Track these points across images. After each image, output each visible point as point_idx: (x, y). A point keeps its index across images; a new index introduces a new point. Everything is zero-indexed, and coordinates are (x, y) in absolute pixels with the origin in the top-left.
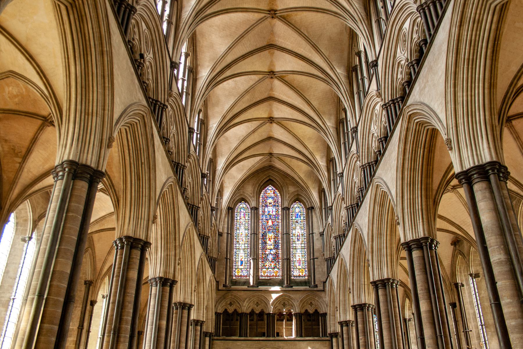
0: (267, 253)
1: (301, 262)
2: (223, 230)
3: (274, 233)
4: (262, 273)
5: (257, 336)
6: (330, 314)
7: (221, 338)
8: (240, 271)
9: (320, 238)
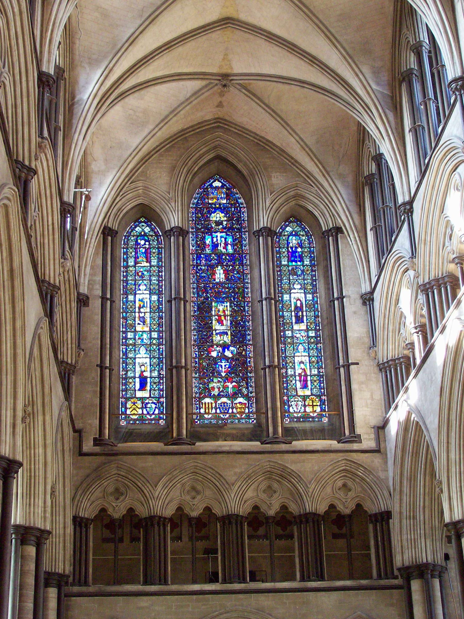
0: (214, 354)
1: (309, 378)
5: (194, 582)
6: (401, 513)
7: (92, 589)
8: (139, 404)
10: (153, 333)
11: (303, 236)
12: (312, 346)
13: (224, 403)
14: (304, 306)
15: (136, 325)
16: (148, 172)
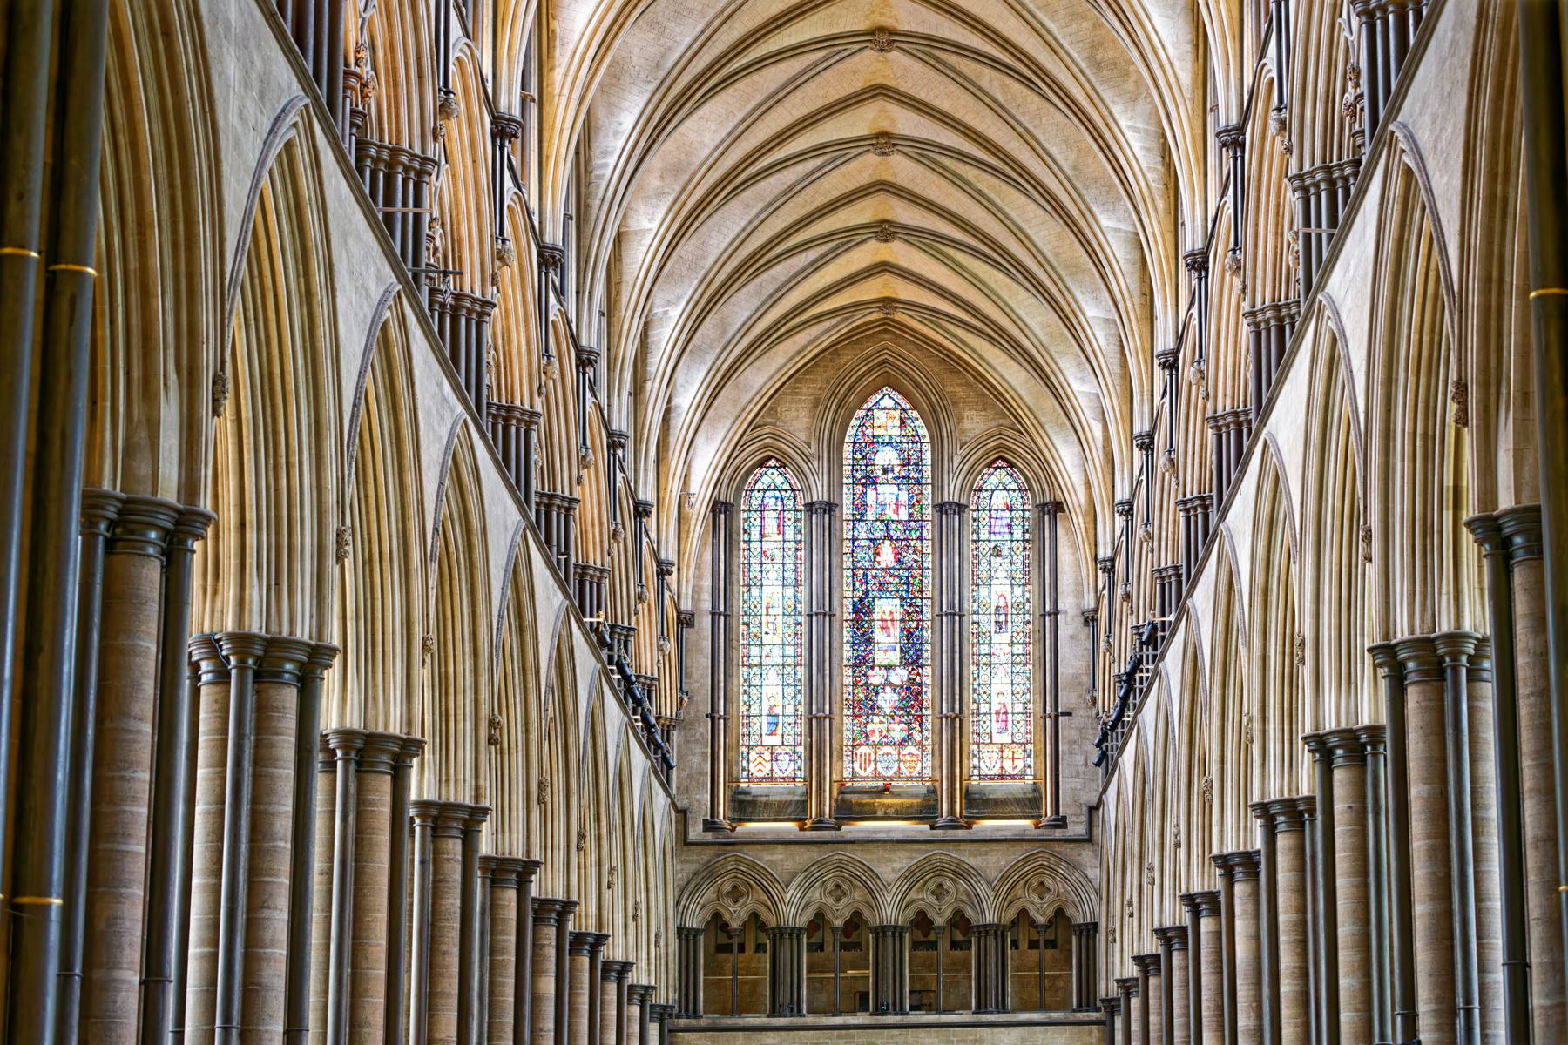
2: (696, 599)
3: (902, 598)
4: (856, 765)
8: (767, 756)
9: (1085, 633)
10: (787, 648)
11: (1014, 491)
12: (1018, 668)
13: (888, 754)
14: (1010, 605)
15: (763, 635)
16: (779, 409)
